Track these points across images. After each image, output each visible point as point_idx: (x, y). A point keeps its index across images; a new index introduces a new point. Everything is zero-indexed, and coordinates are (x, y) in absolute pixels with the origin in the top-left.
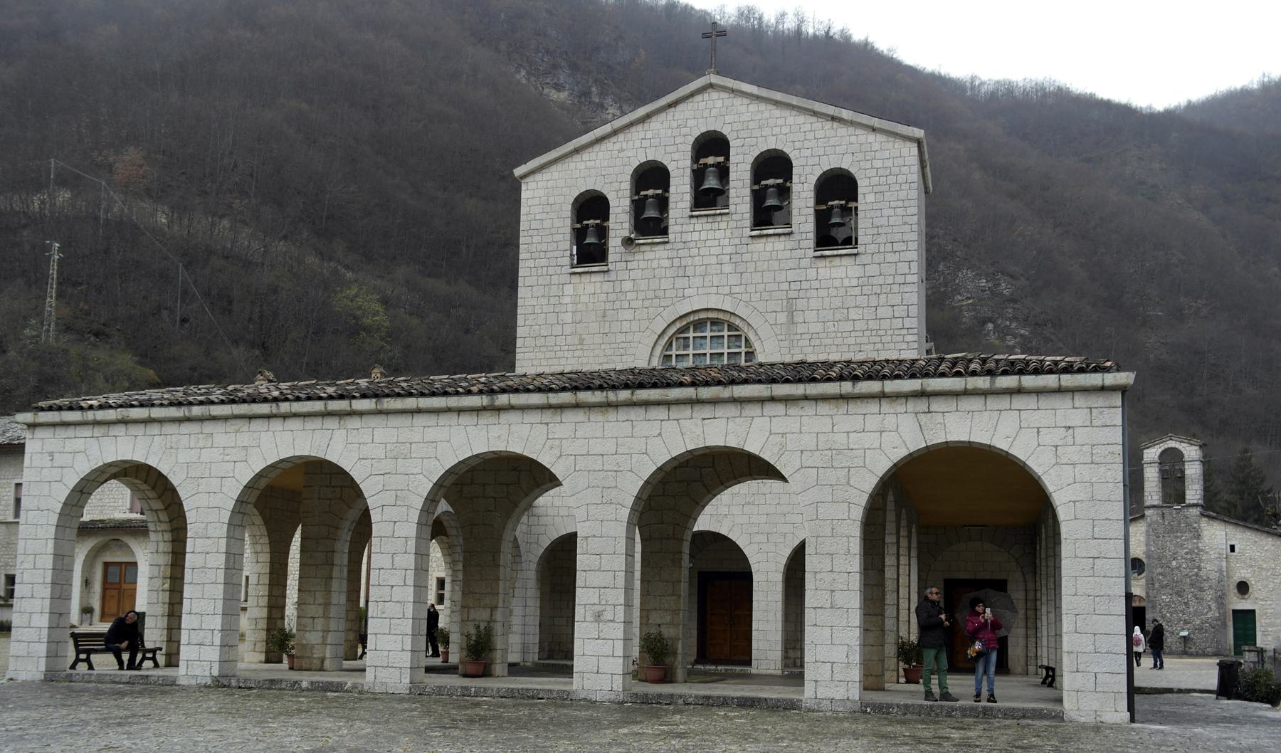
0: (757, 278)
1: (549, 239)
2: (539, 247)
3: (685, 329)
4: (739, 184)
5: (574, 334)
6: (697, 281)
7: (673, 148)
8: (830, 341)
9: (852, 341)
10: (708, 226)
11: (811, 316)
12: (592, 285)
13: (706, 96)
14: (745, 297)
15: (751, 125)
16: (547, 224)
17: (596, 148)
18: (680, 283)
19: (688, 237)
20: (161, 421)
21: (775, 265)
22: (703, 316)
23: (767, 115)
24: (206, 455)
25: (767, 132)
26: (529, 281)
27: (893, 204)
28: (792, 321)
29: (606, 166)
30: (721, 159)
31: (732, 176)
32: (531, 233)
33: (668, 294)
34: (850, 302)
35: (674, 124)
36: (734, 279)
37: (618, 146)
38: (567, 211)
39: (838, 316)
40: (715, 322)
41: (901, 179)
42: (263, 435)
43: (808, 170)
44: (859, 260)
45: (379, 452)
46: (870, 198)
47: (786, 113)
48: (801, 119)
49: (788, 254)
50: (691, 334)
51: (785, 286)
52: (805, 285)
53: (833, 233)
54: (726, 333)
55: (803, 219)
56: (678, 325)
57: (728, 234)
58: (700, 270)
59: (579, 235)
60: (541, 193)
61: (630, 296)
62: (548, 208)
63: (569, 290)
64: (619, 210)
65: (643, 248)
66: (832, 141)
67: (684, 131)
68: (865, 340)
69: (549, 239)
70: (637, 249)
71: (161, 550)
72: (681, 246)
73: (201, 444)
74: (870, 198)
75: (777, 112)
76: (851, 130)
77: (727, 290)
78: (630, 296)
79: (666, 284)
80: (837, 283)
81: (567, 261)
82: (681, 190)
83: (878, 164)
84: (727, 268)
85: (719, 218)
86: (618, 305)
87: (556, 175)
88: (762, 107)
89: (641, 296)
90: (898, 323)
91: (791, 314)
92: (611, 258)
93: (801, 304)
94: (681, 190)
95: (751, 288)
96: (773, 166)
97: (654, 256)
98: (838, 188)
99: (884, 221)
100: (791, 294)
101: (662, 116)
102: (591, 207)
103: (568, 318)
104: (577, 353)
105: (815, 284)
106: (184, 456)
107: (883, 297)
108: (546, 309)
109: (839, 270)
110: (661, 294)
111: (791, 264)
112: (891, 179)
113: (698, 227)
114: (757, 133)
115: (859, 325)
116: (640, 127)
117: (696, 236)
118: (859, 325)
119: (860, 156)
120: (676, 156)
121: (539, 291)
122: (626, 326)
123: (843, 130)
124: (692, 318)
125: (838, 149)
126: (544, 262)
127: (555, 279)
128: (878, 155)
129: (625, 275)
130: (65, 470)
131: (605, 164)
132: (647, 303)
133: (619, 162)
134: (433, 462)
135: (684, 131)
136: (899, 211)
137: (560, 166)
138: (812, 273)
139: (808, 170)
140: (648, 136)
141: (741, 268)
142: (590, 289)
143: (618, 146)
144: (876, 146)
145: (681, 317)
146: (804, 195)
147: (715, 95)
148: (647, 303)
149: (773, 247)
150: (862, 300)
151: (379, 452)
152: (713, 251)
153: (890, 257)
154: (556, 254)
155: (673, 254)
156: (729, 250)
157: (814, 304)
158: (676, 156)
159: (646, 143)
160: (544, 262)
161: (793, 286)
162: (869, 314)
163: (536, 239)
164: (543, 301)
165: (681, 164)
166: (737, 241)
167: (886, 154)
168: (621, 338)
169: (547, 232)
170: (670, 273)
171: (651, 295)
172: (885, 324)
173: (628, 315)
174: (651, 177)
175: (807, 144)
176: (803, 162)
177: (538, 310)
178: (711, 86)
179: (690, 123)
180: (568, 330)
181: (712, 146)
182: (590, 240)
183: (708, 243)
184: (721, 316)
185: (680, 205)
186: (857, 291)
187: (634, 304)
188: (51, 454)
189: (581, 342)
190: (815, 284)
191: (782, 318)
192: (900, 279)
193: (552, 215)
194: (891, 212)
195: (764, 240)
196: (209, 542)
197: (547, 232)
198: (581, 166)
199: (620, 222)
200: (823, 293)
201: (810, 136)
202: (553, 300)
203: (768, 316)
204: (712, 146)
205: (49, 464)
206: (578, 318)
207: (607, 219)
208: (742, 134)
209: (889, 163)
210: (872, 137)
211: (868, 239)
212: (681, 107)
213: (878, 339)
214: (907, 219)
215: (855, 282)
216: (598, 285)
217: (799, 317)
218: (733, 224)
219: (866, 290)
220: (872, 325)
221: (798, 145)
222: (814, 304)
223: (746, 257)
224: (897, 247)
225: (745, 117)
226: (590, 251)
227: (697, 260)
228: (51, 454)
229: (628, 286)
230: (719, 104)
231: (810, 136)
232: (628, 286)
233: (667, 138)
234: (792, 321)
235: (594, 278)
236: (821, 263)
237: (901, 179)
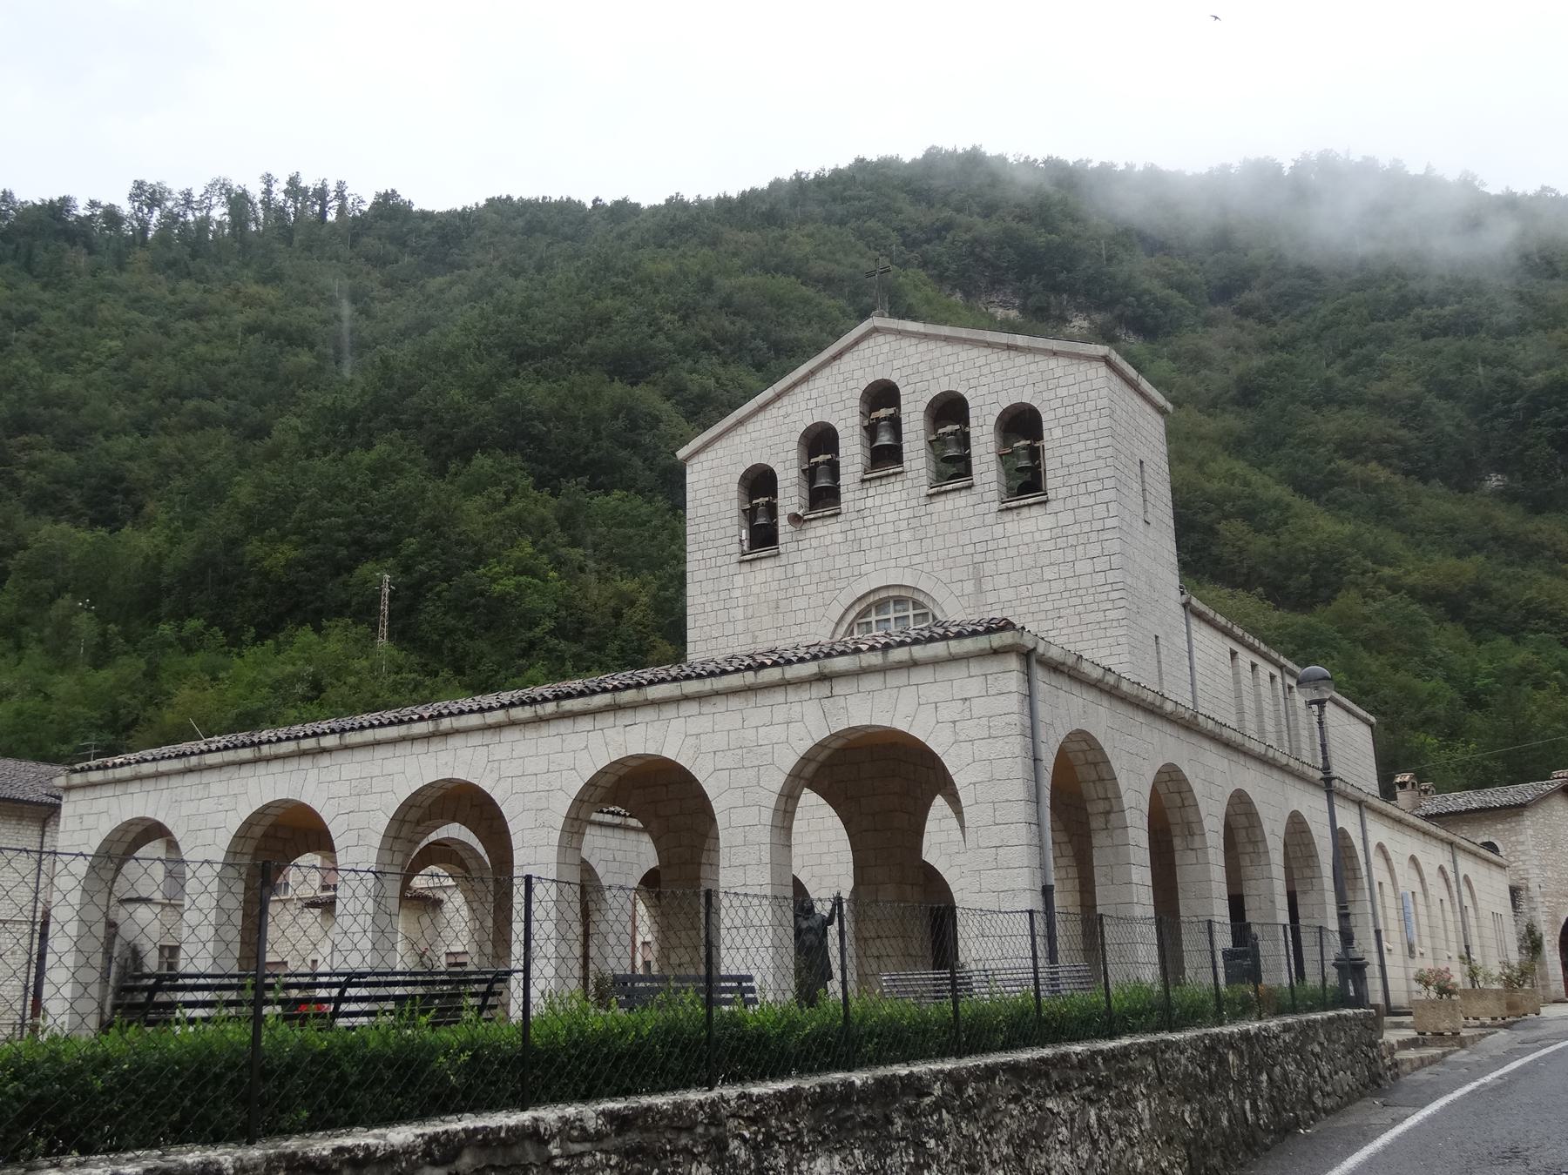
0: (939, 543)
1: (715, 525)
3: (865, 613)
4: (913, 436)
5: (746, 631)
6: (873, 555)
7: (840, 406)
8: (1024, 609)
9: (1049, 606)
10: (881, 490)
11: (1001, 581)
12: (765, 572)
13: (871, 342)
14: (927, 567)
15: (922, 367)
16: (714, 509)
17: (761, 416)
18: (856, 559)
20: (167, 774)
21: (957, 526)
22: (883, 594)
24: (205, 806)
25: (938, 372)
26: (699, 576)
27: (1083, 437)
28: (980, 590)
29: (767, 434)
30: (891, 411)
31: (905, 428)
34: (1044, 559)
35: (840, 378)
36: (913, 548)
37: (782, 412)
38: (734, 489)
40: (898, 601)
41: (1090, 406)
43: (986, 409)
44: (1051, 507)
45: (344, 789)
46: (1057, 433)
47: (957, 348)
48: (974, 353)
50: (873, 618)
52: (992, 545)
54: (911, 613)
55: (984, 467)
56: (857, 609)
57: (904, 496)
58: (876, 542)
59: (750, 514)
60: (706, 474)
62: (714, 491)
65: (814, 524)
66: (1010, 373)
67: (852, 384)
68: (1064, 603)
69: (715, 525)
70: (807, 525)
74: (1057, 433)
75: (948, 349)
76: (1030, 357)
77: (906, 561)
79: (840, 562)
80: (1027, 539)
81: (735, 548)
82: (852, 453)
83: (1063, 392)
84: (906, 536)
85: (893, 479)
86: (790, 593)
87: (720, 453)
88: (932, 345)
89: (815, 579)
90: (1100, 578)
91: (979, 581)
92: (781, 539)
93: (989, 568)
94: (852, 453)
96: (949, 410)
97: (825, 532)
98: (1021, 424)
99: (1073, 459)
101: (827, 371)
102: (759, 482)
103: (739, 613)
106: (186, 809)
107: (1080, 548)
108: (716, 606)
109: (1031, 523)
110: (835, 574)
111: (975, 522)
112: (1079, 408)
115: (1056, 586)
116: (804, 387)
118: (1056, 586)
119: (1042, 386)
120: (843, 414)
121: (708, 586)
122: (800, 616)
123: (1021, 360)
124: (872, 599)
125: (1018, 382)
126: (713, 552)
128: (1062, 382)
131: (770, 433)
132: (821, 588)
133: (784, 429)
134: (390, 796)
135: (852, 384)
136: (1092, 444)
137: (724, 442)
138: (998, 530)
139: (986, 409)
143: (782, 412)
144: (1059, 372)
145: (859, 599)
146: (983, 439)
147: (881, 339)
148: (821, 588)
149: (955, 504)
150: (1057, 556)
151: (344, 789)
152: (890, 517)
153: (1084, 500)
154: (725, 541)
155: (846, 526)
156: (906, 514)
157: (1004, 566)
158: (843, 414)
159: (812, 404)
161: (979, 548)
162: (1066, 571)
163: (703, 527)
164: (713, 597)
165: (850, 422)
166: (914, 503)
167: (1071, 380)
170: (844, 548)
171: (825, 576)
172: (1086, 581)
173: (801, 603)
174: (820, 440)
175: (984, 380)
176: (979, 401)
178: (876, 330)
180: (740, 627)
181: (882, 396)
182: (761, 521)
183: (884, 509)
184: (903, 593)
185: (851, 469)
186: (1050, 545)
190: (1004, 543)
191: (969, 587)
192: (1098, 525)
193: (718, 498)
194: (1081, 446)
195: (943, 498)
198: (746, 438)
199: (790, 497)
200: (1012, 552)
201: (985, 370)
204: (882, 396)
207: (775, 496)
208: (914, 379)
209: (1075, 390)
210: (1053, 363)
212: (847, 357)
213: (1079, 601)
214: (1100, 453)
215: (1047, 535)
217: (987, 585)
218: (908, 483)
219: (1061, 543)
220: (1071, 584)
221: (973, 383)
222: (1004, 566)
224: (1092, 487)
226: (762, 537)
230: (886, 348)
232: (800, 569)
233: (829, 393)
234: (980, 590)
235: (765, 564)
236: (1008, 517)
237: (1090, 406)
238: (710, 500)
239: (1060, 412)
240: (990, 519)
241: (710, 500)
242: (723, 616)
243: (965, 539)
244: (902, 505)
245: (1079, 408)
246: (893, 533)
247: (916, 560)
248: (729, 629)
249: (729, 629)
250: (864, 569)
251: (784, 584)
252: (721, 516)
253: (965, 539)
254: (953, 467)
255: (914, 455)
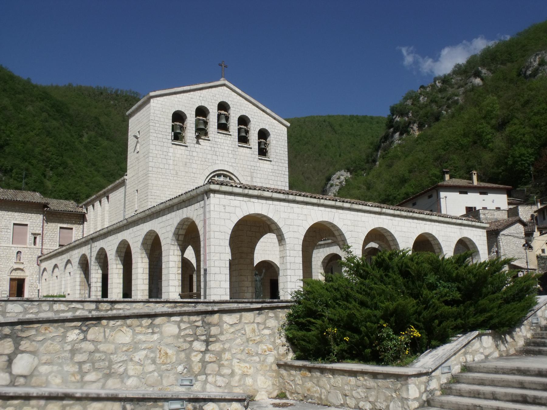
1: (162, 126)
2: (159, 129)
4: (234, 124)
5: (174, 169)
6: (220, 158)
7: (211, 104)
10: (224, 138)
12: (178, 150)
14: (237, 168)
16: (162, 120)
18: (215, 157)
19: (217, 140)
22: (222, 172)
23: (242, 102)
32: (155, 121)
33: (210, 161)
34: (270, 177)
36: (233, 160)
37: (190, 96)
39: (266, 182)
40: (225, 176)
42: (312, 211)
43: (256, 126)
46: (274, 142)
49: (250, 155)
51: (250, 167)
53: (263, 152)
56: (213, 174)
58: (221, 154)
60: (160, 106)
61: (196, 158)
63: (171, 150)
64: (191, 122)
69: (162, 126)
71: (176, 254)
72: (214, 143)
73: (289, 211)
77: (230, 164)
78: (196, 158)
79: (209, 157)
80: (266, 170)
83: (276, 131)
84: (231, 156)
89: (200, 159)
91: (252, 177)
93: (255, 175)
95: (239, 165)
96: (243, 121)
98: (263, 134)
100: (252, 171)
103: (171, 162)
104: (175, 178)
105: (259, 169)
108: (162, 156)
110: (207, 160)
113: (220, 137)
114: (239, 107)
117: (219, 140)
119: (271, 127)
120: (212, 107)
121: (159, 148)
122: (194, 171)
124: (217, 172)
125: (265, 122)
127: (165, 144)
129: (193, 149)
130: (231, 214)
131: (186, 101)
132: (202, 163)
137: (167, 97)
138: (258, 164)
139: (256, 126)
140: (202, 96)
141: (235, 157)
142: (180, 152)
143: (190, 96)
144: (276, 125)
147: (225, 88)
150: (273, 178)
155: (212, 145)
156: (231, 149)
159: (201, 98)
160: (161, 136)
164: (161, 153)
166: (234, 146)
167: (278, 128)
168: (192, 175)
169: (162, 123)
170: (211, 152)
171: (203, 160)
173: (194, 166)
175: (255, 117)
177: (158, 156)
179: (217, 96)
181: (223, 106)
183: (224, 144)
186: (271, 174)
187: (197, 162)
188: (224, 206)
189: (177, 174)
192: (283, 173)
193: (164, 117)
196: (296, 252)
197: (162, 123)
201: (256, 114)
202: (165, 153)
203: (245, 177)
205: (223, 210)
206: (175, 163)
208: (234, 106)
209: (279, 132)
211: (274, 156)
215: (271, 171)
216: (183, 151)
217: (254, 180)
223: (237, 153)
225: (235, 100)
227: (220, 150)
228: (224, 206)
229: (195, 154)
231: (256, 114)
238: (161, 116)
239: (275, 136)
240: (256, 160)
241: (161, 116)
242: (164, 161)
243: (248, 163)
244: (230, 145)
245: (280, 137)
246: (222, 151)
247: (234, 164)
248: (167, 166)
249: (167, 166)
250: (217, 162)
251: (189, 157)
252: (165, 123)
253: (248, 163)
254: (243, 139)
255: (234, 131)
